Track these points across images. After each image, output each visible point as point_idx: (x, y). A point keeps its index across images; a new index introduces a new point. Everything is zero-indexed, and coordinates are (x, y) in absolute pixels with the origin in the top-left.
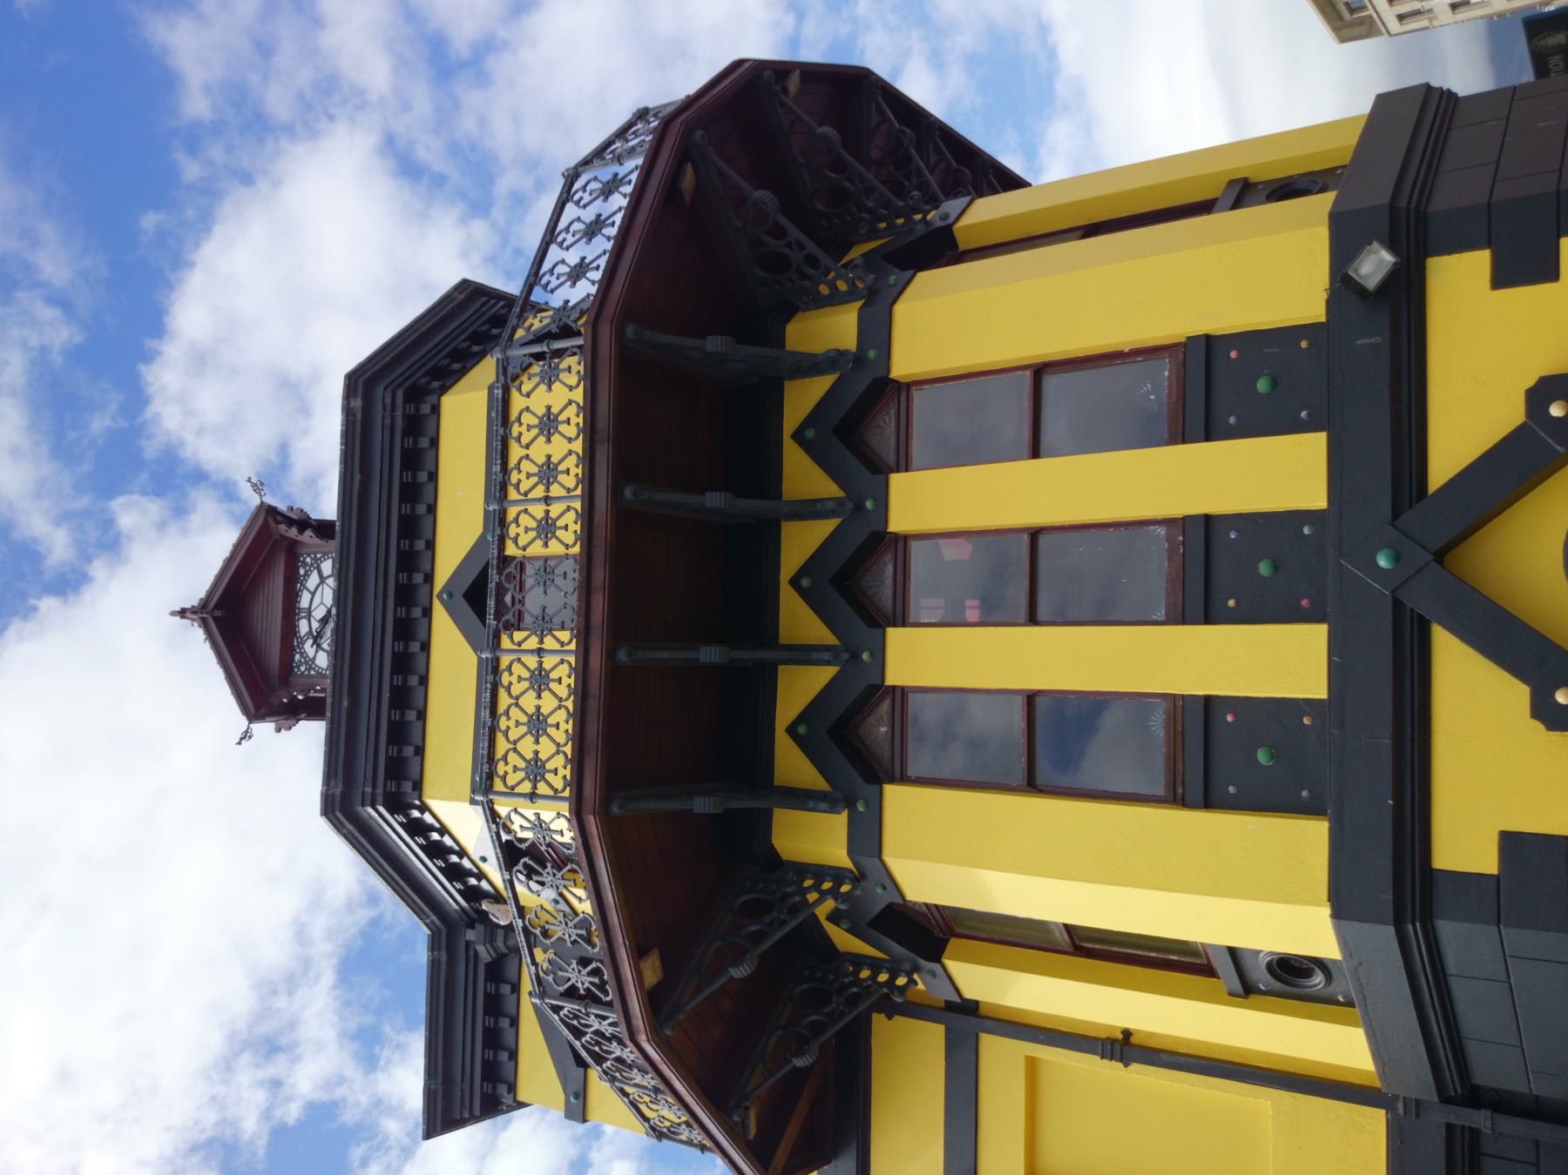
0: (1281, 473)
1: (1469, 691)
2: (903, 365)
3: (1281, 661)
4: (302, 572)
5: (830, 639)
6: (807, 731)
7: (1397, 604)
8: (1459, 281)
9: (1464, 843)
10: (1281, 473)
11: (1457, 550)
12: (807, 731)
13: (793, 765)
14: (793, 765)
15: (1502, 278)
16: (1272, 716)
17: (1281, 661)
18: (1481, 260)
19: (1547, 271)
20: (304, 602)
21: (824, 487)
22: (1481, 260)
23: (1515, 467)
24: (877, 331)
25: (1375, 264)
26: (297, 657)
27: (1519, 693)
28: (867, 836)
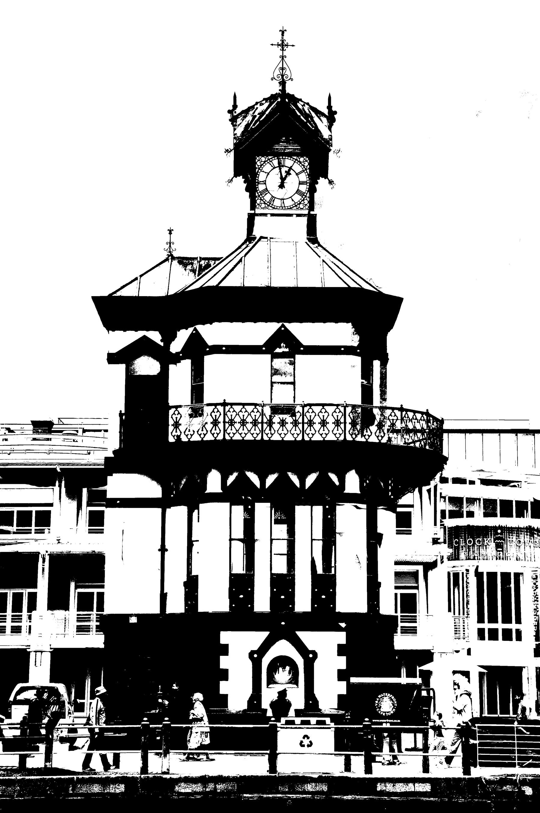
0: (303, 602)
1: (256, 638)
3: (262, 602)
4: (302, 159)
5: (267, 485)
8: (341, 638)
9: (225, 637)
10: (303, 602)
15: (339, 646)
16: (250, 597)
17: (262, 602)
18: (344, 642)
19: (340, 654)
22: (344, 642)
24: (352, 498)
25: (343, 625)
26: (263, 159)
27: (256, 648)
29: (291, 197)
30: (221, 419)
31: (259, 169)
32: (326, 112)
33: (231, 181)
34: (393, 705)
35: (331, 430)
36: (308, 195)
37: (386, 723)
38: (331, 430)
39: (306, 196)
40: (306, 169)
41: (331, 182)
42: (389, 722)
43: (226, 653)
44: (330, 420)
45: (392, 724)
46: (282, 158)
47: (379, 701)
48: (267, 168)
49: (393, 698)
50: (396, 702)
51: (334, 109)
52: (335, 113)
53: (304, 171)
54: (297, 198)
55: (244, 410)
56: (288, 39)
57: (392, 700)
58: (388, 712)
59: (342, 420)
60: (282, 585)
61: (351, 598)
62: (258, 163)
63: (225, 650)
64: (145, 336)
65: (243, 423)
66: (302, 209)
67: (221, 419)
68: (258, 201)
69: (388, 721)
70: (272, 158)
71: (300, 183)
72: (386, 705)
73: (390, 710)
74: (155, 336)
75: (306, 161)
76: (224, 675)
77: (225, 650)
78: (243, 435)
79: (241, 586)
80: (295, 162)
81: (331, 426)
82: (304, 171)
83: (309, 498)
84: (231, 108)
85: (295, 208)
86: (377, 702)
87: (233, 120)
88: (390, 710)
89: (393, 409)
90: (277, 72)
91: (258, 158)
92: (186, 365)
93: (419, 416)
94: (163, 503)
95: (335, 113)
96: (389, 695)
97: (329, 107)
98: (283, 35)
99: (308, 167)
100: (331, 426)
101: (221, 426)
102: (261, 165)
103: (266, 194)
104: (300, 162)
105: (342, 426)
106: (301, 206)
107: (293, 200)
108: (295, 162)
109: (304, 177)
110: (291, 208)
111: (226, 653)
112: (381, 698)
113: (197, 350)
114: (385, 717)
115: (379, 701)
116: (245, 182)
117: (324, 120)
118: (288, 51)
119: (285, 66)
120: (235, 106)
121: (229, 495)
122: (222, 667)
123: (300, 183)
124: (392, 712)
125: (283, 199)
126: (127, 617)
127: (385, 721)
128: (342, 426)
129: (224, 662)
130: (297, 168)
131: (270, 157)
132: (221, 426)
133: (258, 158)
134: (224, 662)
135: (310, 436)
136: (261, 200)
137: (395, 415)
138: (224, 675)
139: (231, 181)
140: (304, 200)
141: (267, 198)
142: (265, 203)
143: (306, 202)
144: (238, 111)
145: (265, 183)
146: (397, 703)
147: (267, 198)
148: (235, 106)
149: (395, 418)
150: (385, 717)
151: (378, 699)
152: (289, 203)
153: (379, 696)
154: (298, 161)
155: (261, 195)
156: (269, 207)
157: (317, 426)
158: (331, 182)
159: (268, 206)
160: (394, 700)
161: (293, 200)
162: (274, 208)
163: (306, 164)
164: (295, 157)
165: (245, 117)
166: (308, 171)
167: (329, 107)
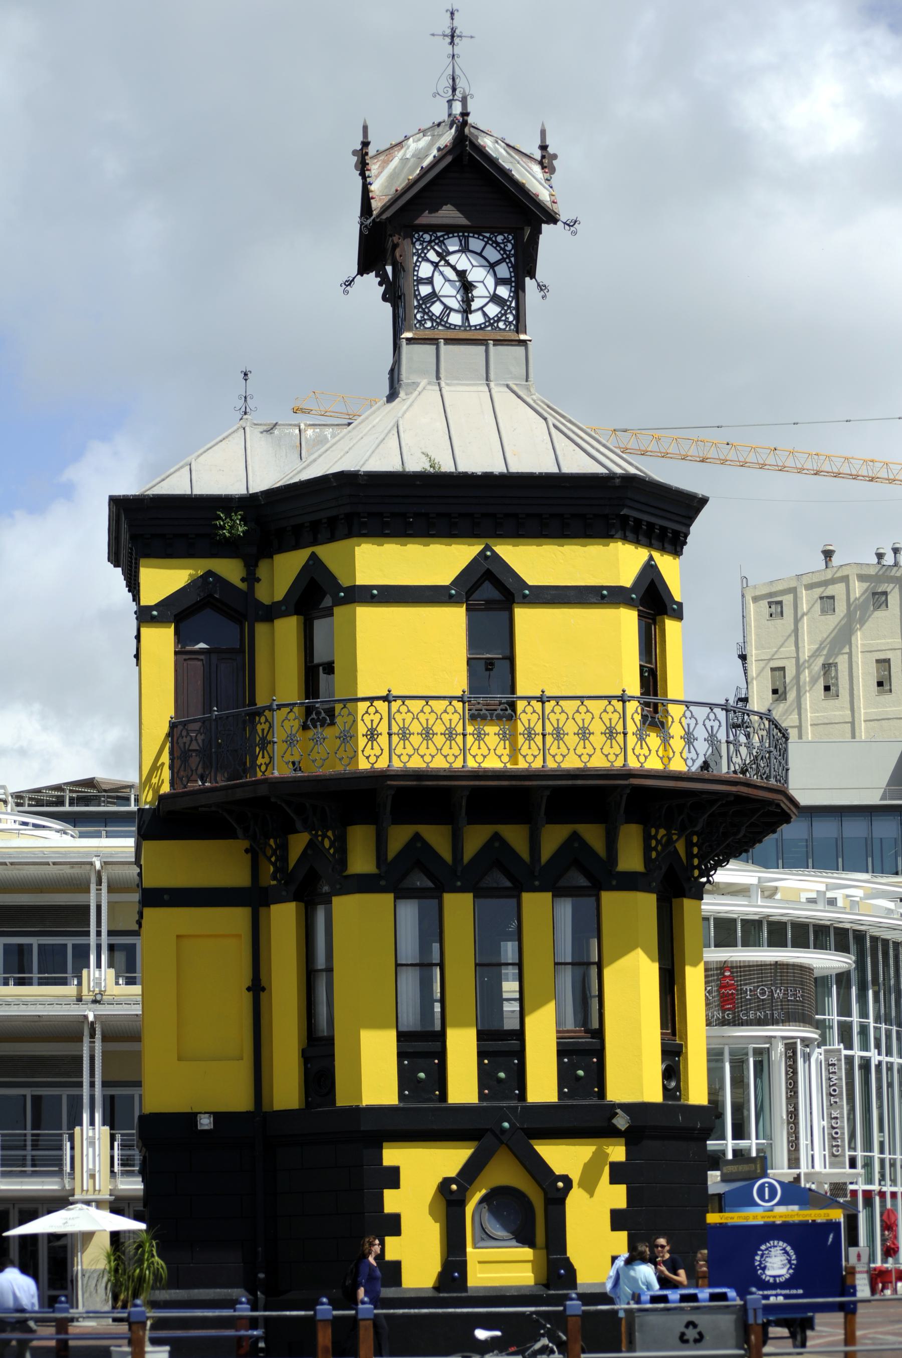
0: (542, 1085)
2: (608, 898)
3: (463, 1086)
4: (500, 238)
6: (417, 842)
7: (487, 1130)
10: (542, 1085)
11: (507, 1150)
12: (417, 842)
13: (399, 837)
14: (399, 837)
17: (463, 1086)
20: (475, 244)
21: (548, 849)
23: (540, 1170)
24: (630, 882)
27: (453, 1173)
28: (365, 884)
29: (481, 309)
30: (383, 728)
31: (419, 256)
32: (538, 155)
33: (349, 283)
34: (789, 1261)
35: (598, 747)
36: (513, 305)
37: (776, 1295)
38: (598, 747)
39: (509, 307)
40: (509, 257)
41: (541, 287)
42: (781, 1295)
43: (396, 1185)
44: (597, 727)
45: (786, 1297)
46: (463, 236)
47: (762, 1256)
49: (788, 1248)
50: (794, 1257)
51: (551, 150)
52: (555, 157)
54: (493, 310)
55: (427, 709)
57: (786, 1253)
58: (779, 1276)
59: (620, 728)
60: (502, 1051)
61: (633, 1076)
63: (392, 1178)
64: (209, 573)
65: (427, 734)
66: (504, 330)
67: (383, 728)
69: (779, 1291)
70: (442, 236)
72: (776, 1263)
73: (783, 1271)
74: (230, 570)
75: (509, 241)
76: (393, 1225)
77: (392, 1178)
78: (428, 758)
79: (421, 1053)
80: (487, 243)
81: (598, 739)
83: (551, 879)
84: (359, 147)
85: (489, 328)
86: (758, 1258)
87: (363, 167)
88: (783, 1271)
89: (711, 706)
90: (447, 83)
91: (416, 235)
92: (288, 629)
94: (255, 899)
95: (555, 157)
96: (781, 1243)
97: (544, 148)
99: (513, 252)
100: (598, 739)
101: (383, 740)
103: (433, 303)
104: (498, 244)
106: (501, 325)
107: (485, 314)
108: (487, 243)
109: (503, 271)
110: (481, 329)
111: (395, 1184)
112: (767, 1249)
113: (320, 596)
114: (775, 1286)
115: (762, 1256)
116: (380, 284)
117: (537, 169)
118: (461, 46)
119: (458, 72)
120: (366, 144)
121: (390, 879)
122: (389, 1208)
124: (787, 1276)
126: (192, 1117)
127: (774, 1292)
128: (620, 738)
129: (392, 1201)
130: (493, 254)
131: (439, 234)
132: (383, 740)
133: (416, 235)
134: (392, 1201)
135: (559, 758)
136: (424, 313)
137: (716, 718)
138: (393, 1225)
139: (349, 283)
140: (505, 314)
143: (511, 318)
144: (372, 151)
145: (430, 281)
146: (797, 1259)
147: (437, 309)
148: (366, 144)
149: (717, 723)
150: (775, 1286)
151: (760, 1253)
152: (476, 319)
153: (763, 1247)
154: (494, 242)
155: (424, 303)
156: (440, 328)
157: (571, 740)
158: (541, 287)
159: (439, 324)
160: (792, 1252)
161: (485, 314)
162: (449, 328)
163: (509, 247)
164: (488, 235)
165: (386, 163)
166: (513, 259)
167: (544, 148)
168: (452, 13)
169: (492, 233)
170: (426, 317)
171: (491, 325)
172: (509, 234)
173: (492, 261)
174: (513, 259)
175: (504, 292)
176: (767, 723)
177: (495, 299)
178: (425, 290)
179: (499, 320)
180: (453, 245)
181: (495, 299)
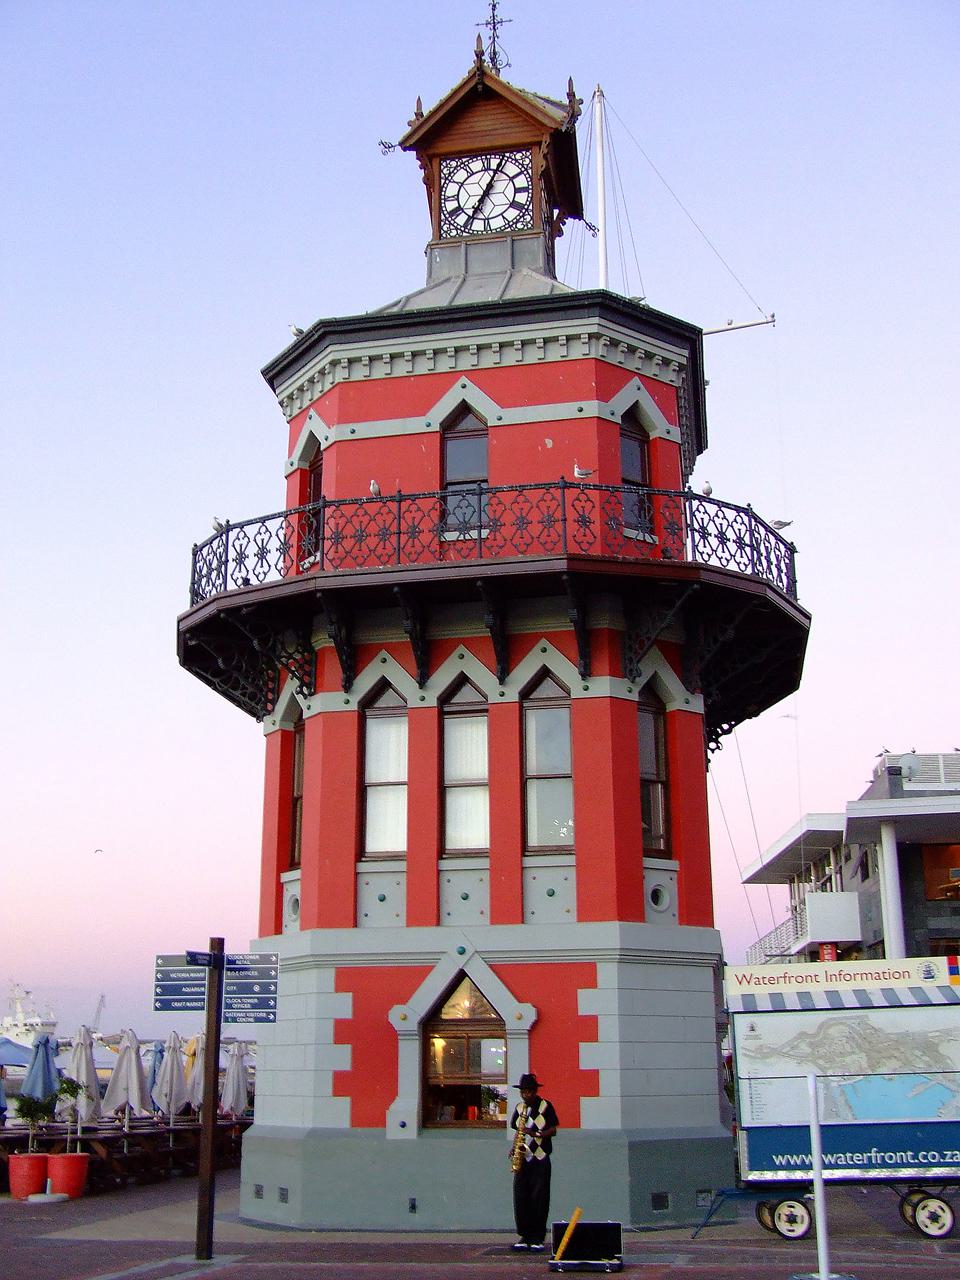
4: (519, 156)
26: (454, 164)
29: (501, 214)
31: (446, 179)
32: (566, 102)
36: (531, 207)
39: (527, 210)
40: (526, 170)
48: (461, 175)
53: (522, 173)
54: (512, 214)
56: (500, 14)
59: (559, 515)
62: (445, 171)
68: (445, 228)
71: (517, 190)
82: (522, 173)
85: (509, 229)
91: (444, 164)
93: (731, 514)
97: (571, 95)
98: (494, 10)
102: (450, 174)
104: (516, 161)
105: (559, 526)
106: (520, 226)
107: (504, 218)
123: (517, 190)
125: (488, 219)
131: (464, 160)
133: (444, 164)
136: (450, 224)
140: (524, 215)
141: (461, 219)
142: (456, 229)
143: (528, 218)
145: (457, 197)
156: (465, 234)
158: (591, 227)
161: (504, 218)
166: (530, 171)
167: (571, 95)
168: (494, 6)
169: (511, 152)
170: (452, 227)
171: (510, 226)
172: (527, 151)
173: (511, 176)
174: (530, 171)
175: (522, 198)
176: (746, 519)
177: (514, 204)
178: (451, 206)
179: (518, 221)
180: (476, 165)
181: (514, 204)
